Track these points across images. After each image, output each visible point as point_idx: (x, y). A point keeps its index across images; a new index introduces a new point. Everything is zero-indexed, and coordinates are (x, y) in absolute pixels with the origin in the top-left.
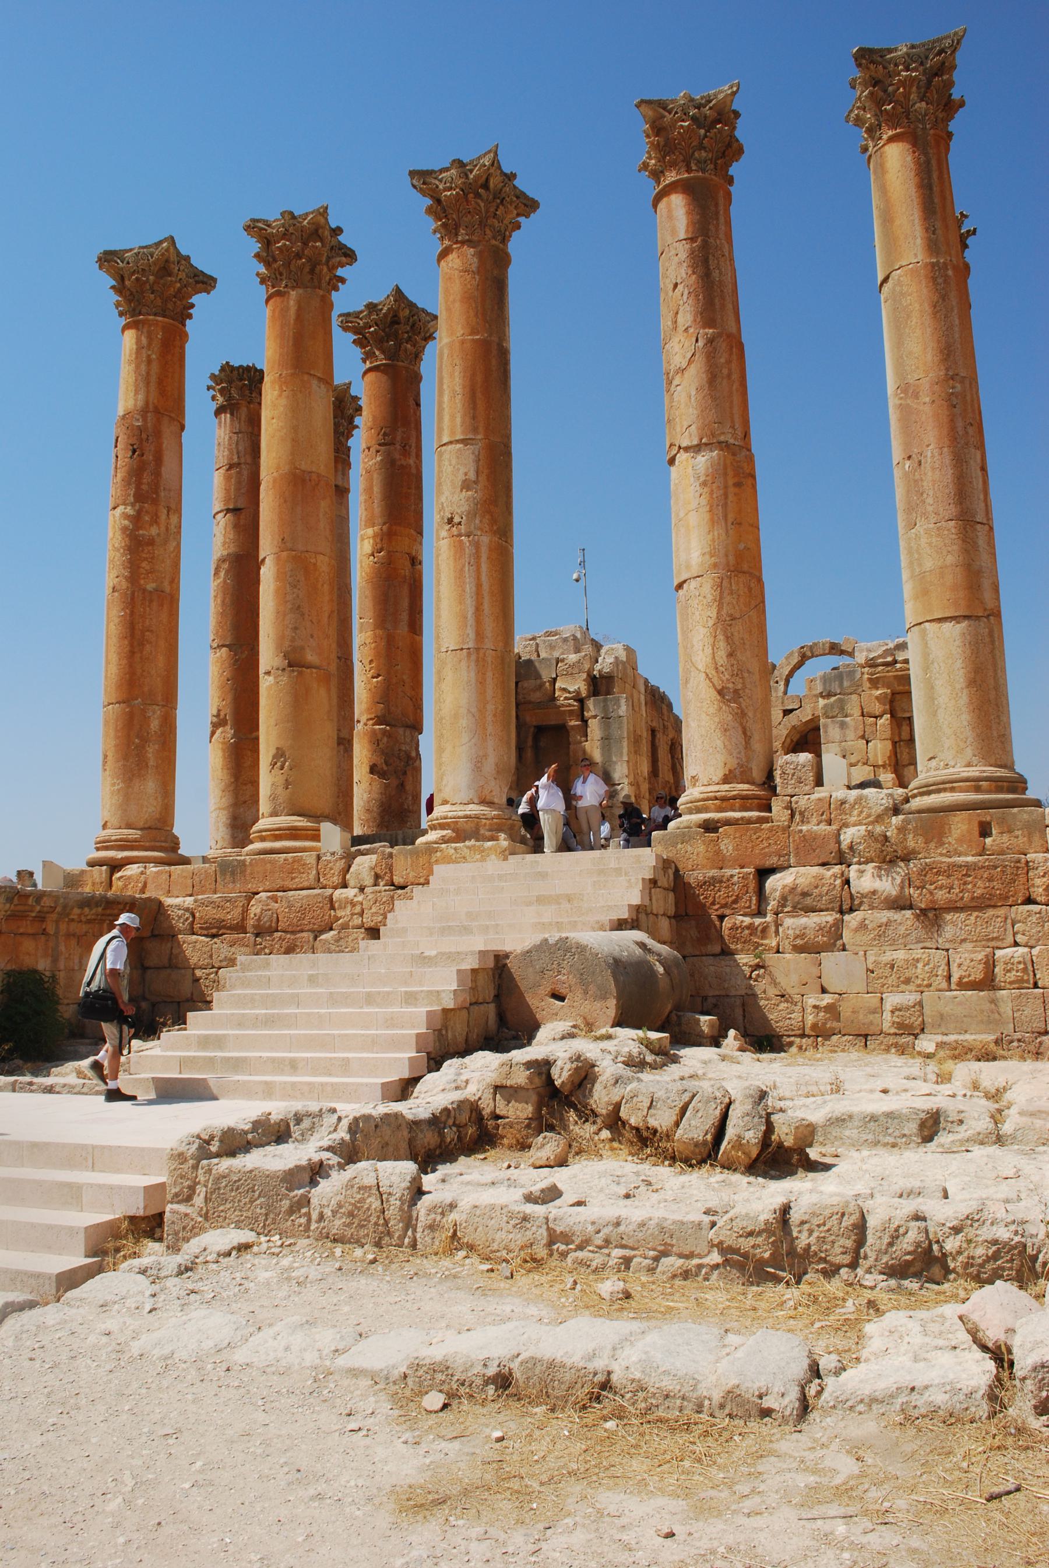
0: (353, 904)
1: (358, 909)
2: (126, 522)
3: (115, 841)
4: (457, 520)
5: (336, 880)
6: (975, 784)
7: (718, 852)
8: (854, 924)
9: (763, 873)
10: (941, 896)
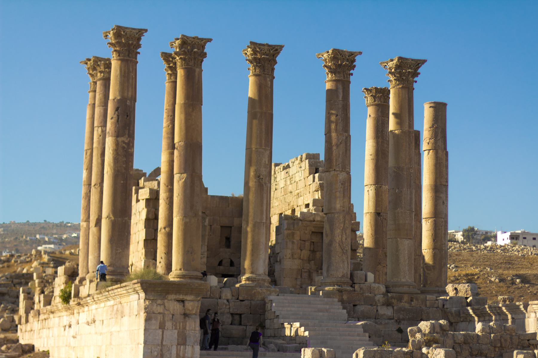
0: (226, 305)
1: (228, 307)
2: (124, 145)
4: (261, 177)
5: (217, 296)
6: (409, 286)
7: (343, 298)
8: (379, 323)
9: (354, 306)
10: (401, 317)
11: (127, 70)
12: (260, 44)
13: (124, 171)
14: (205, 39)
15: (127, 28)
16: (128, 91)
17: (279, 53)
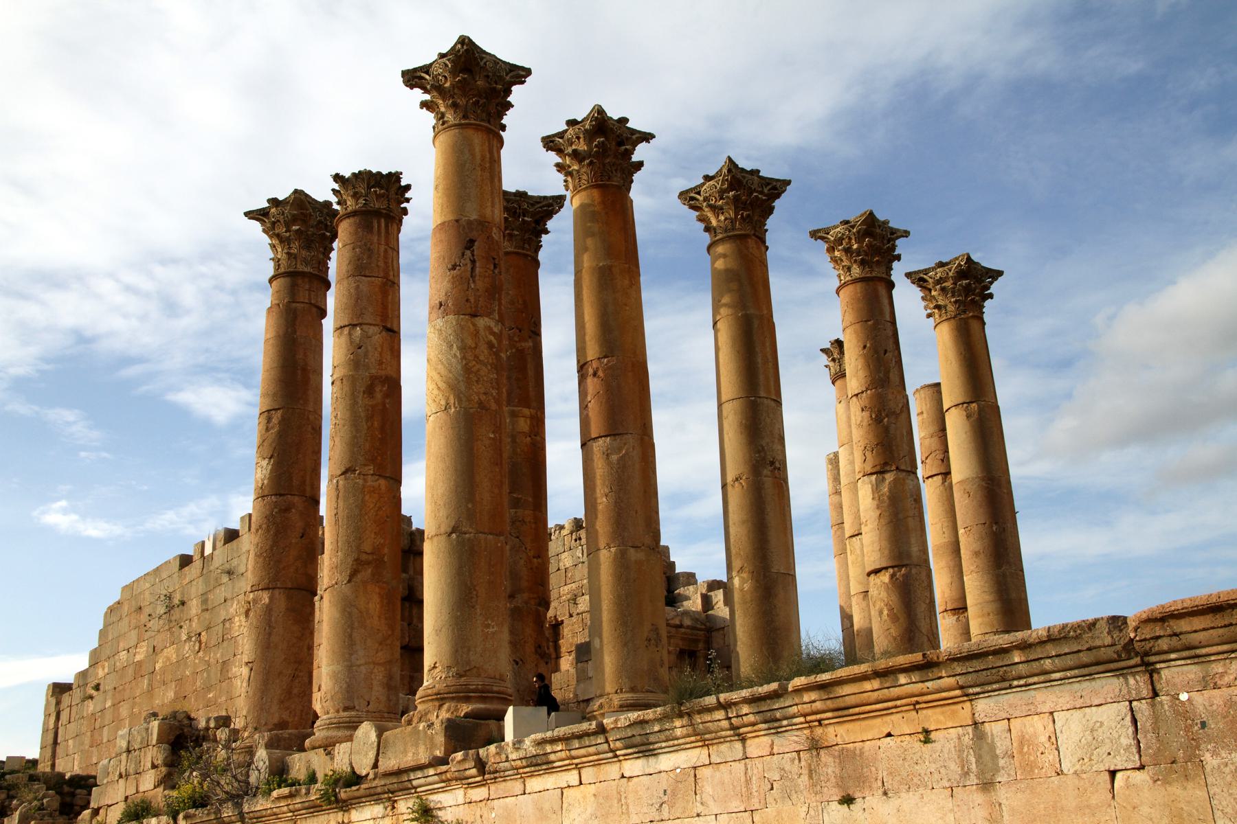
2: (492, 338)
3: (498, 692)
4: (777, 465)
11: (488, 156)
12: (743, 169)
13: (494, 406)
14: (640, 132)
15: (484, 52)
16: (493, 206)
17: (778, 196)
